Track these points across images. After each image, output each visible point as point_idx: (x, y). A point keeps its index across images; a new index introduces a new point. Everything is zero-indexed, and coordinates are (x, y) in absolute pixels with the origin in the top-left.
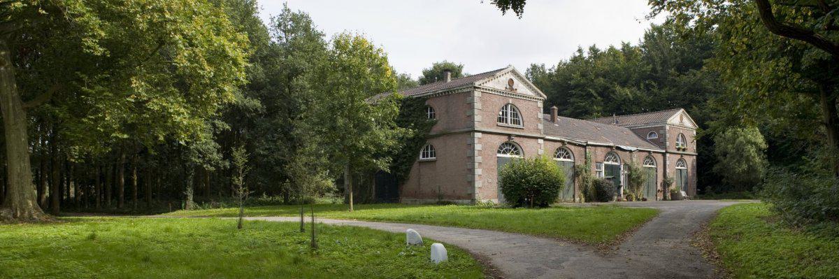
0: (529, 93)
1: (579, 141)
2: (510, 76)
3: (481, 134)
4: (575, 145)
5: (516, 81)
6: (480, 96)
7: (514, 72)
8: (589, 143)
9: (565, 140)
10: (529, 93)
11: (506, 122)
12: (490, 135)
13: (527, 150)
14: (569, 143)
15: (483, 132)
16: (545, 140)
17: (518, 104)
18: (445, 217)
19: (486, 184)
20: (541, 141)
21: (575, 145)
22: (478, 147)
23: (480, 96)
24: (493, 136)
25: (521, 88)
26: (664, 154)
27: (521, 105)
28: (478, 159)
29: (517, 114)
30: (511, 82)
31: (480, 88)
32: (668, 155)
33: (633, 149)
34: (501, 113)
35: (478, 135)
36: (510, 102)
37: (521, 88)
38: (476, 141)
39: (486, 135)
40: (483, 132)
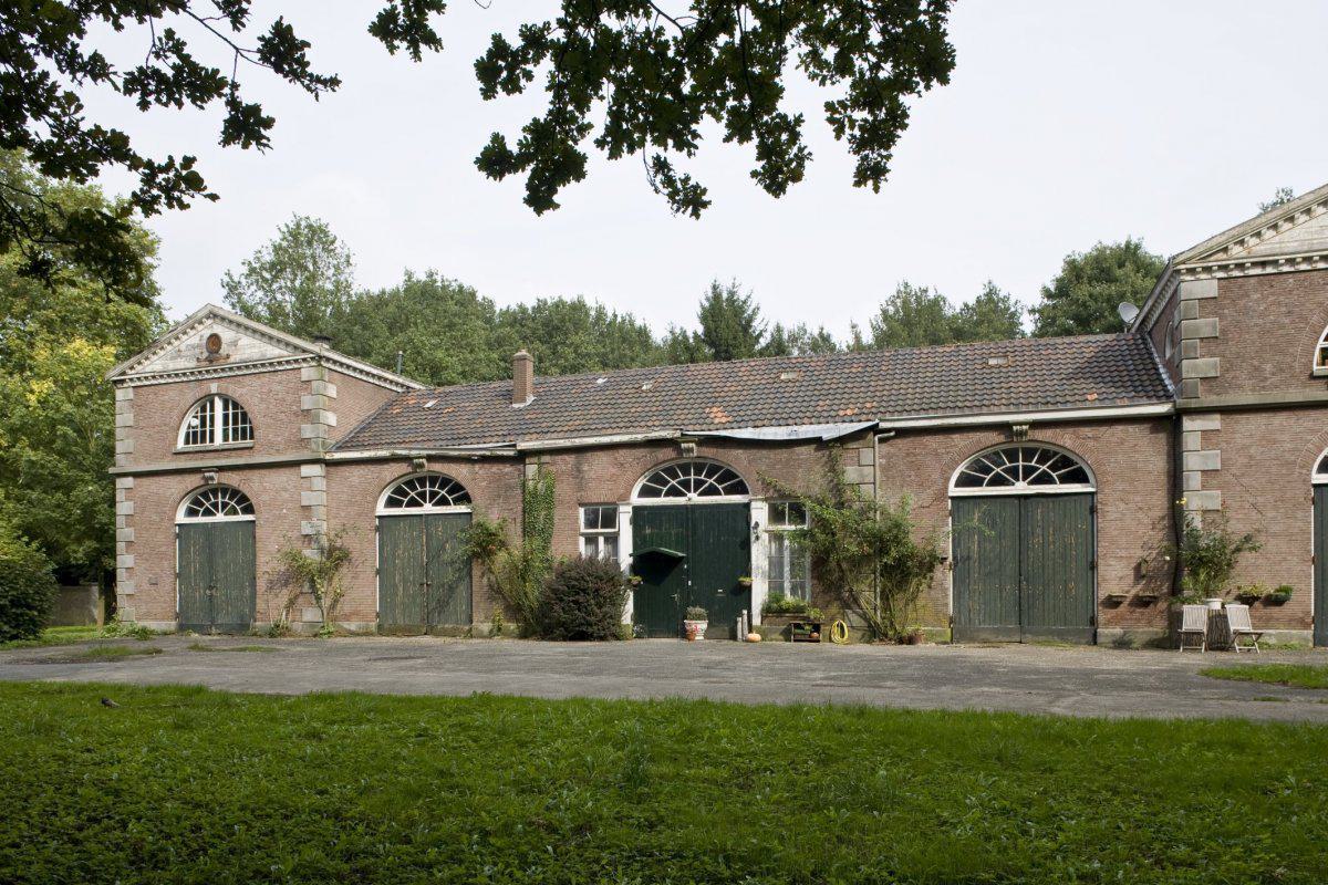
0: (273, 351)
1: (490, 446)
2: (205, 331)
3: (131, 479)
4: (468, 460)
5: (226, 334)
6: (131, 396)
7: (213, 315)
8: (523, 445)
9: (414, 453)
10: (273, 351)
11: (212, 440)
12: (157, 479)
13: (265, 497)
14: (430, 458)
15: (136, 475)
16: (330, 464)
17: (235, 391)
18: (1017, 671)
19: (146, 586)
20: (317, 470)
21: (468, 460)
22: (124, 507)
23: (131, 396)
24: (162, 480)
25: (245, 347)
26: (1169, 426)
27: (248, 393)
28: (124, 532)
29: (244, 415)
30: (215, 340)
31: (123, 381)
32: (1188, 424)
33: (828, 431)
34: (196, 422)
35: (122, 483)
36: (214, 390)
37: (245, 347)
38: (120, 496)
39: (145, 481)
40: (136, 475)
